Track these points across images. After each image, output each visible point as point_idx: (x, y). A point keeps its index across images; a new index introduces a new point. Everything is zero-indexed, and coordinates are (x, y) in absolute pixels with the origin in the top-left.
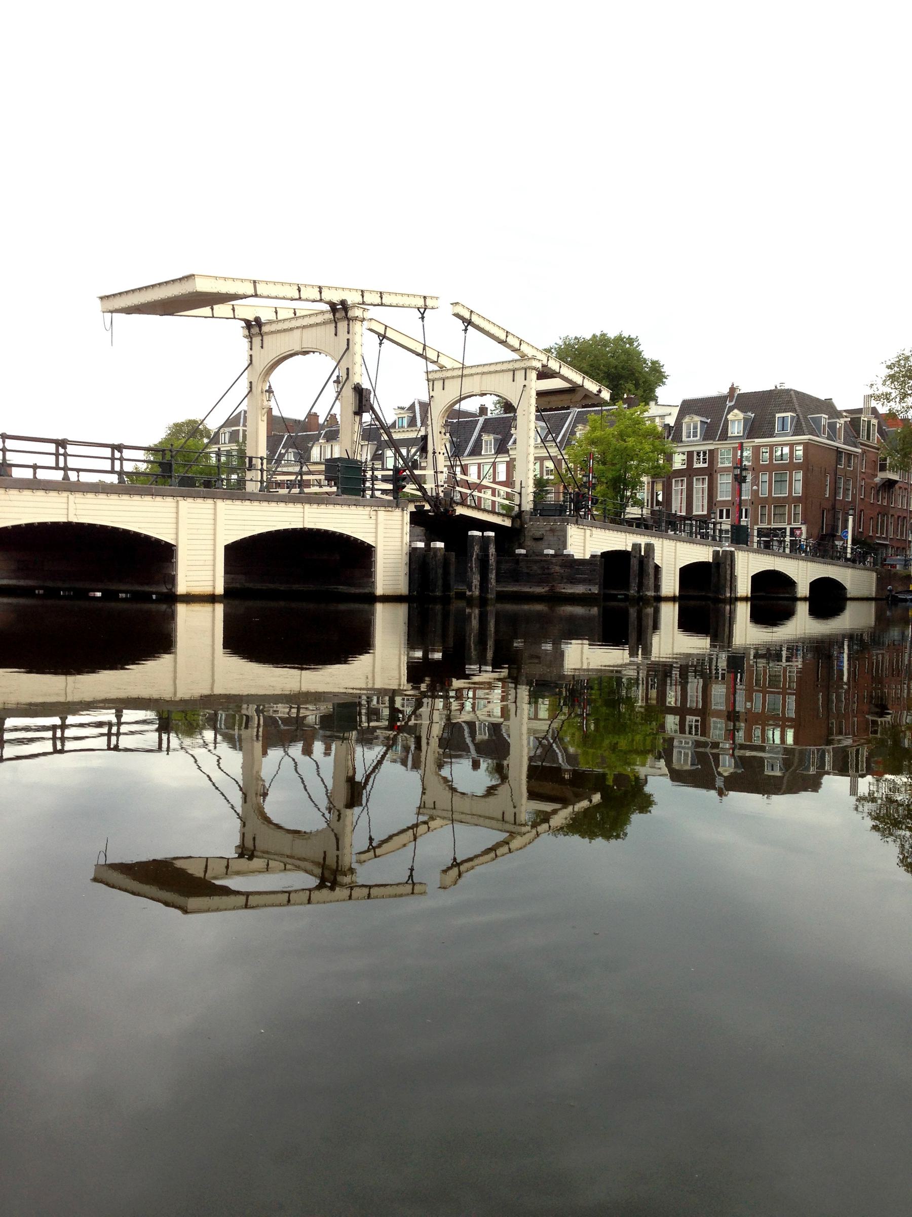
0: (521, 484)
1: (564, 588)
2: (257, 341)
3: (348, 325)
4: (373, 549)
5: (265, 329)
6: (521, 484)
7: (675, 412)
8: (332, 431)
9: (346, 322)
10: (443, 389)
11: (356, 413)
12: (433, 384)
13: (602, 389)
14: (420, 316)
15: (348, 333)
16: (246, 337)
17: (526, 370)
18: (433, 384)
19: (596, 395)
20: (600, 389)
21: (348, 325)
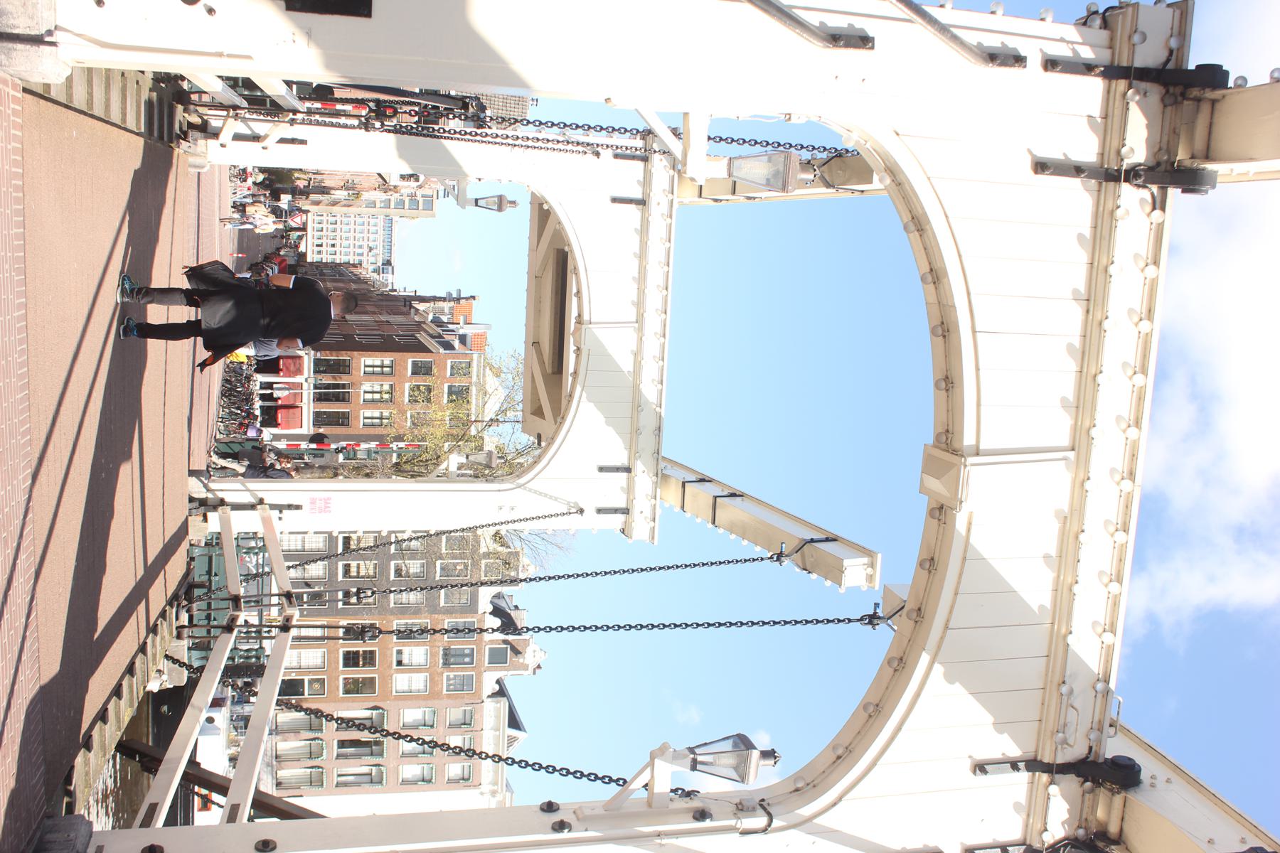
0: (290, 507)
5: (1132, 197)
6: (290, 507)
10: (614, 200)
17: (626, 511)
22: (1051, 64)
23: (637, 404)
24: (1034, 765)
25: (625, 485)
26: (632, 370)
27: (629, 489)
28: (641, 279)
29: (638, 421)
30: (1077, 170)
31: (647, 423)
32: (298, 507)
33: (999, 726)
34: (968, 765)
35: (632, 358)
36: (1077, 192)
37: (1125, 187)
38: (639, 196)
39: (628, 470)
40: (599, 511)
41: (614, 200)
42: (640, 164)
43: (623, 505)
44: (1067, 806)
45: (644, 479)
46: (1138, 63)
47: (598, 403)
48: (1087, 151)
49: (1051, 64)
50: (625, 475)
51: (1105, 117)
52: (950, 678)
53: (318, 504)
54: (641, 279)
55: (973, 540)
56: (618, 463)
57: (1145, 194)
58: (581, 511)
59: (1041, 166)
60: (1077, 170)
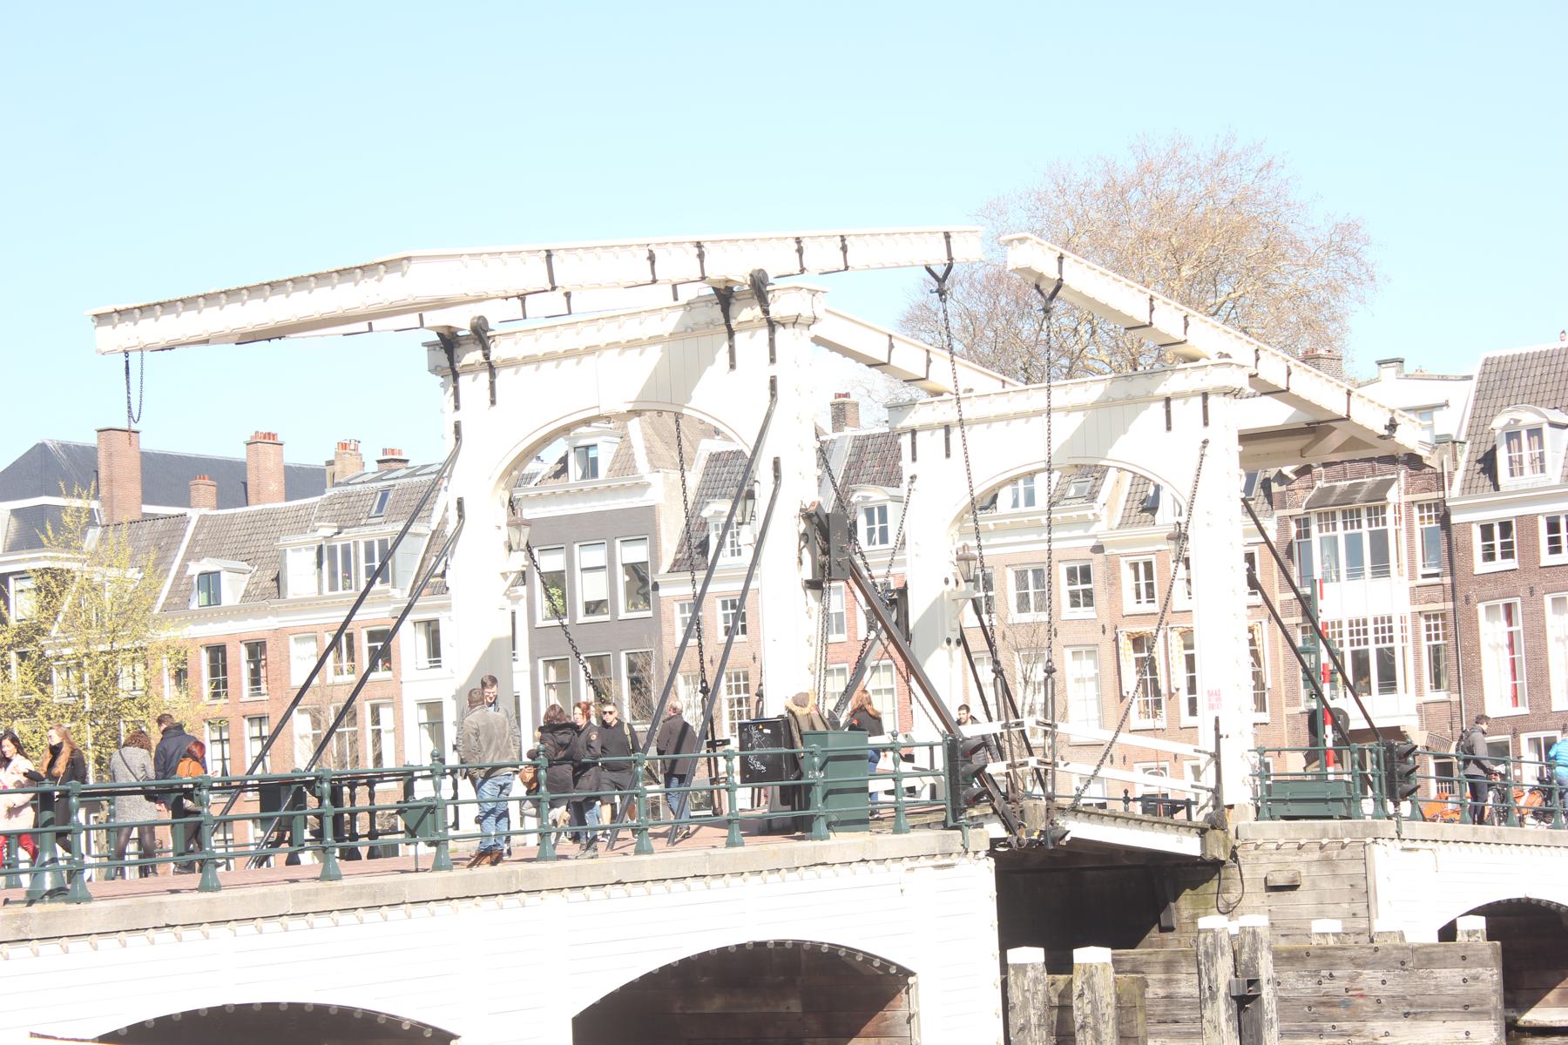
0: (1217, 729)
1: (1387, 1034)
2: (473, 386)
3: (772, 341)
4: (911, 980)
6: (1217, 729)
7: (1462, 397)
8: (348, 496)
9: (764, 333)
11: (814, 585)
12: (914, 444)
13: (1398, 420)
14: (935, 285)
15: (773, 360)
16: (435, 370)
17: (1205, 396)
18: (914, 444)
19: (1381, 437)
20: (1392, 420)
21: (772, 341)
22: (457, 408)
23: (1105, 403)
24: (731, 333)
25: (1182, 401)
26: (1082, 413)
27: (1184, 396)
28: (1005, 418)
29: (1121, 399)
30: (492, 384)
31: (1123, 388)
32: (1217, 720)
33: (712, 361)
34: (733, 373)
35: (1072, 414)
36: (503, 376)
37: (492, 358)
38: (942, 432)
39: (1168, 400)
40: (1206, 424)
41: (948, 455)
42: (919, 435)
43: (1200, 399)
44: (745, 310)
45: (1173, 383)
46: (448, 364)
47: (1111, 444)
48: (485, 376)
49: (457, 408)
50: (1173, 403)
51: (472, 372)
52: (689, 399)
53: (1214, 701)
54: (1005, 418)
55: (633, 399)
56: (1164, 411)
57: (492, 346)
58: (1205, 442)
59: (493, 402)
60: (492, 384)
